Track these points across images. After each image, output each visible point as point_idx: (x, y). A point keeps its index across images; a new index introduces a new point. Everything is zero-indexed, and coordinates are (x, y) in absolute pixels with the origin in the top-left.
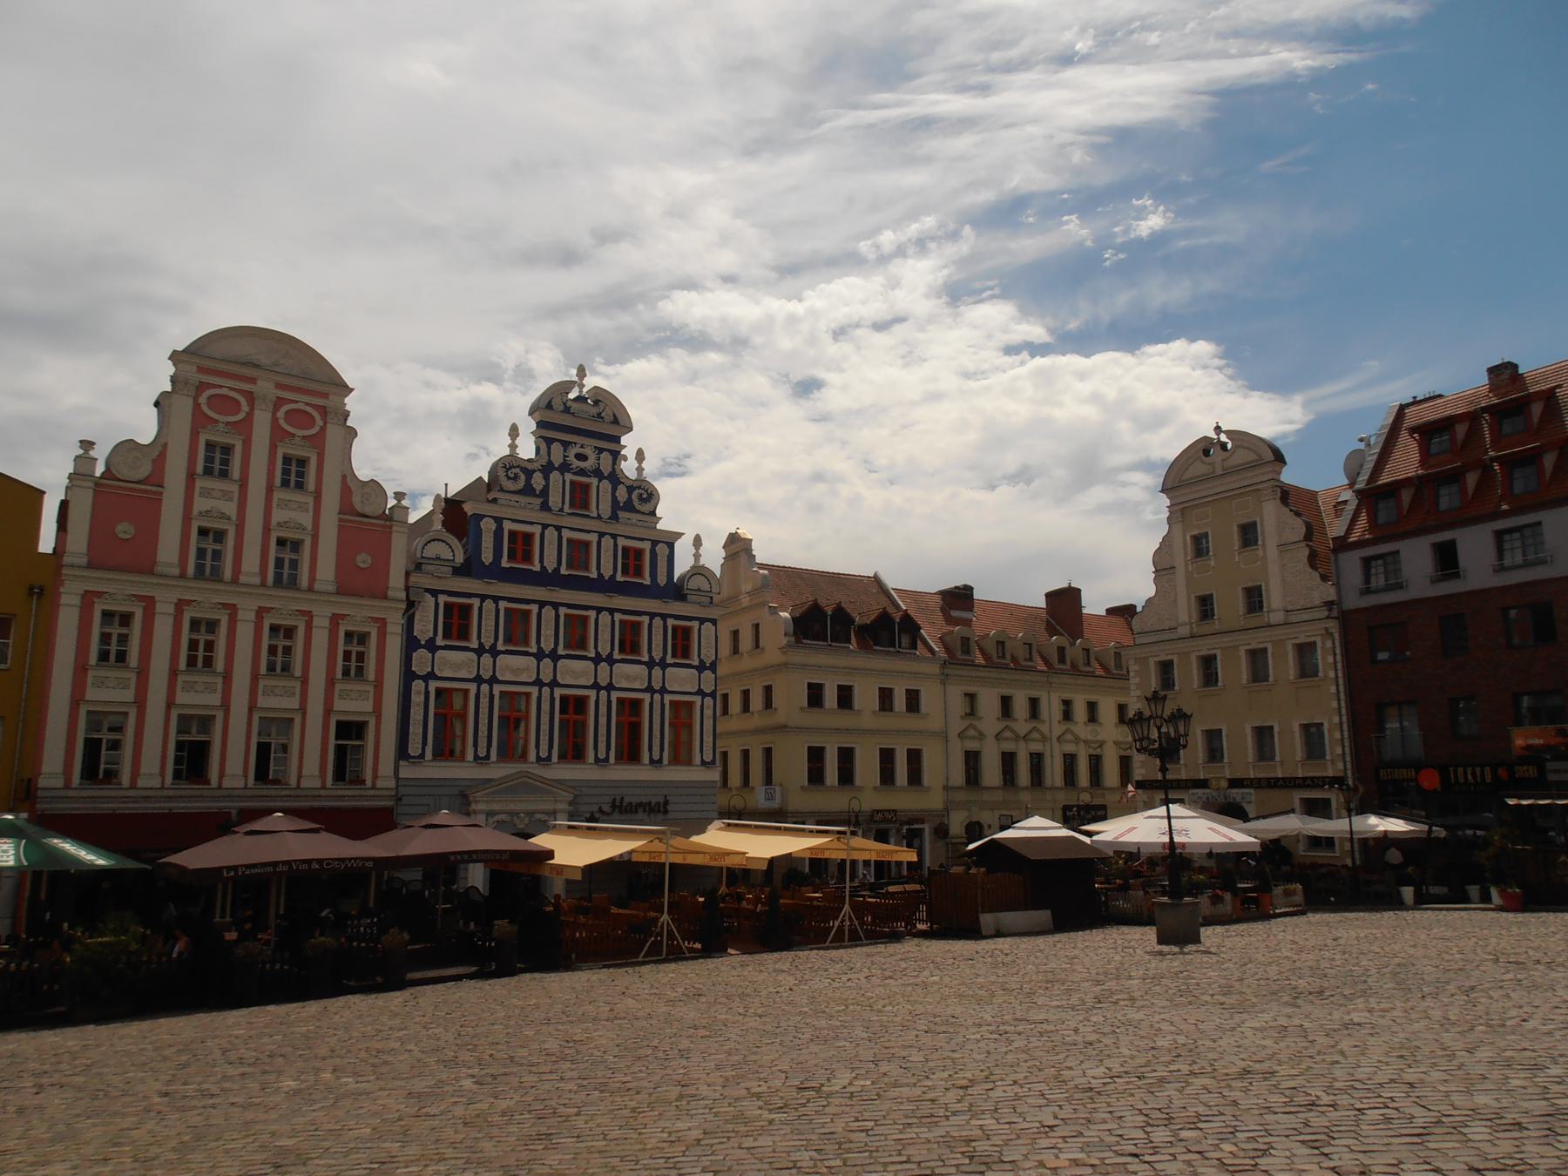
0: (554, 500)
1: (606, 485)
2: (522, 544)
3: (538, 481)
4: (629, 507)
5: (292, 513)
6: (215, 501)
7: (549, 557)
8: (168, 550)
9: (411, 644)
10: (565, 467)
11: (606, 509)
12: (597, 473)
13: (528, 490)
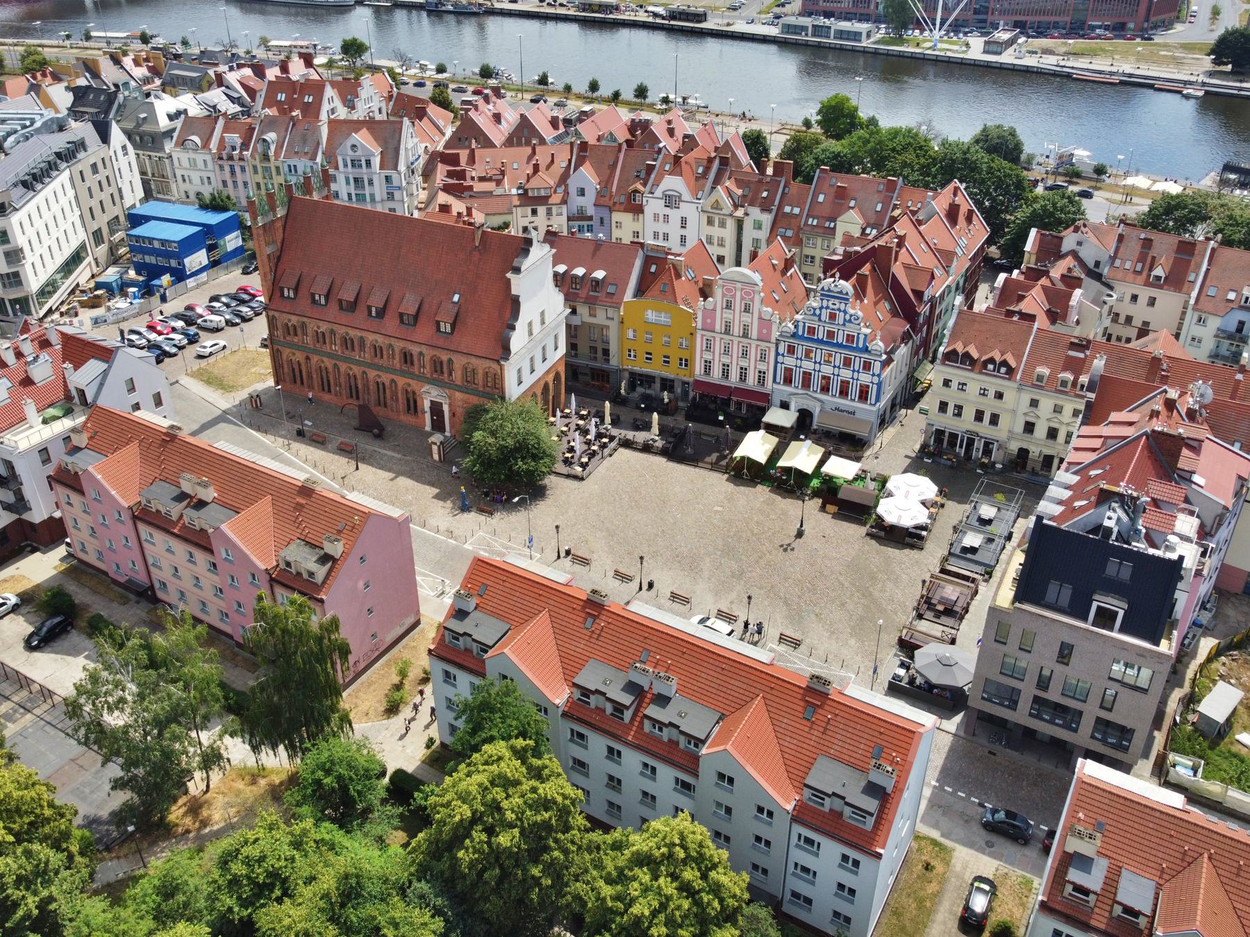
0: (823, 318)
1: (842, 314)
2: (812, 330)
3: (818, 312)
4: (850, 321)
5: (746, 318)
6: (728, 315)
7: (821, 335)
8: (718, 328)
9: (777, 354)
10: (827, 308)
11: (841, 322)
12: (839, 310)
13: (814, 314)
